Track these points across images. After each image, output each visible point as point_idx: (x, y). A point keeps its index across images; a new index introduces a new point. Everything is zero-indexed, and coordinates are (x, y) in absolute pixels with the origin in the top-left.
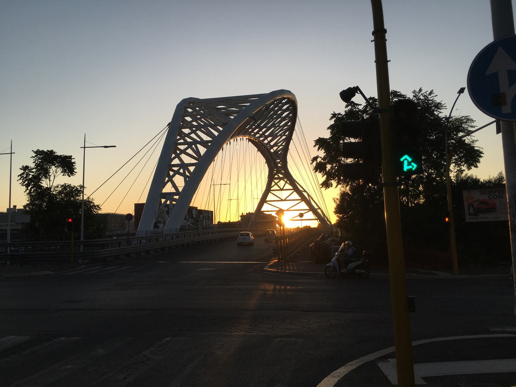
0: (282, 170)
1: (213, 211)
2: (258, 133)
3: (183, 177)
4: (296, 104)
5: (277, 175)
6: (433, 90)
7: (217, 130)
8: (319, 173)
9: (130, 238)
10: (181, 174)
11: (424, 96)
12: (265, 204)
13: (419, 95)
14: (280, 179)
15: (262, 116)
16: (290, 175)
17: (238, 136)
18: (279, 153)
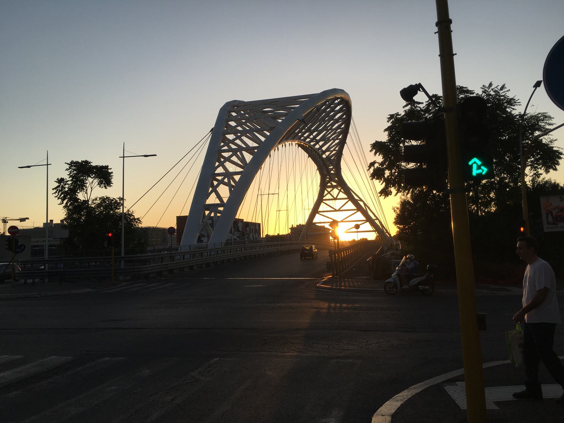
0: (335, 178)
1: (260, 224)
2: (308, 137)
3: (228, 187)
5: (330, 183)
6: (504, 84)
7: (264, 135)
8: (376, 180)
9: (173, 253)
10: (225, 184)
11: (495, 91)
12: (317, 214)
13: (489, 90)
14: (333, 187)
17: (287, 141)
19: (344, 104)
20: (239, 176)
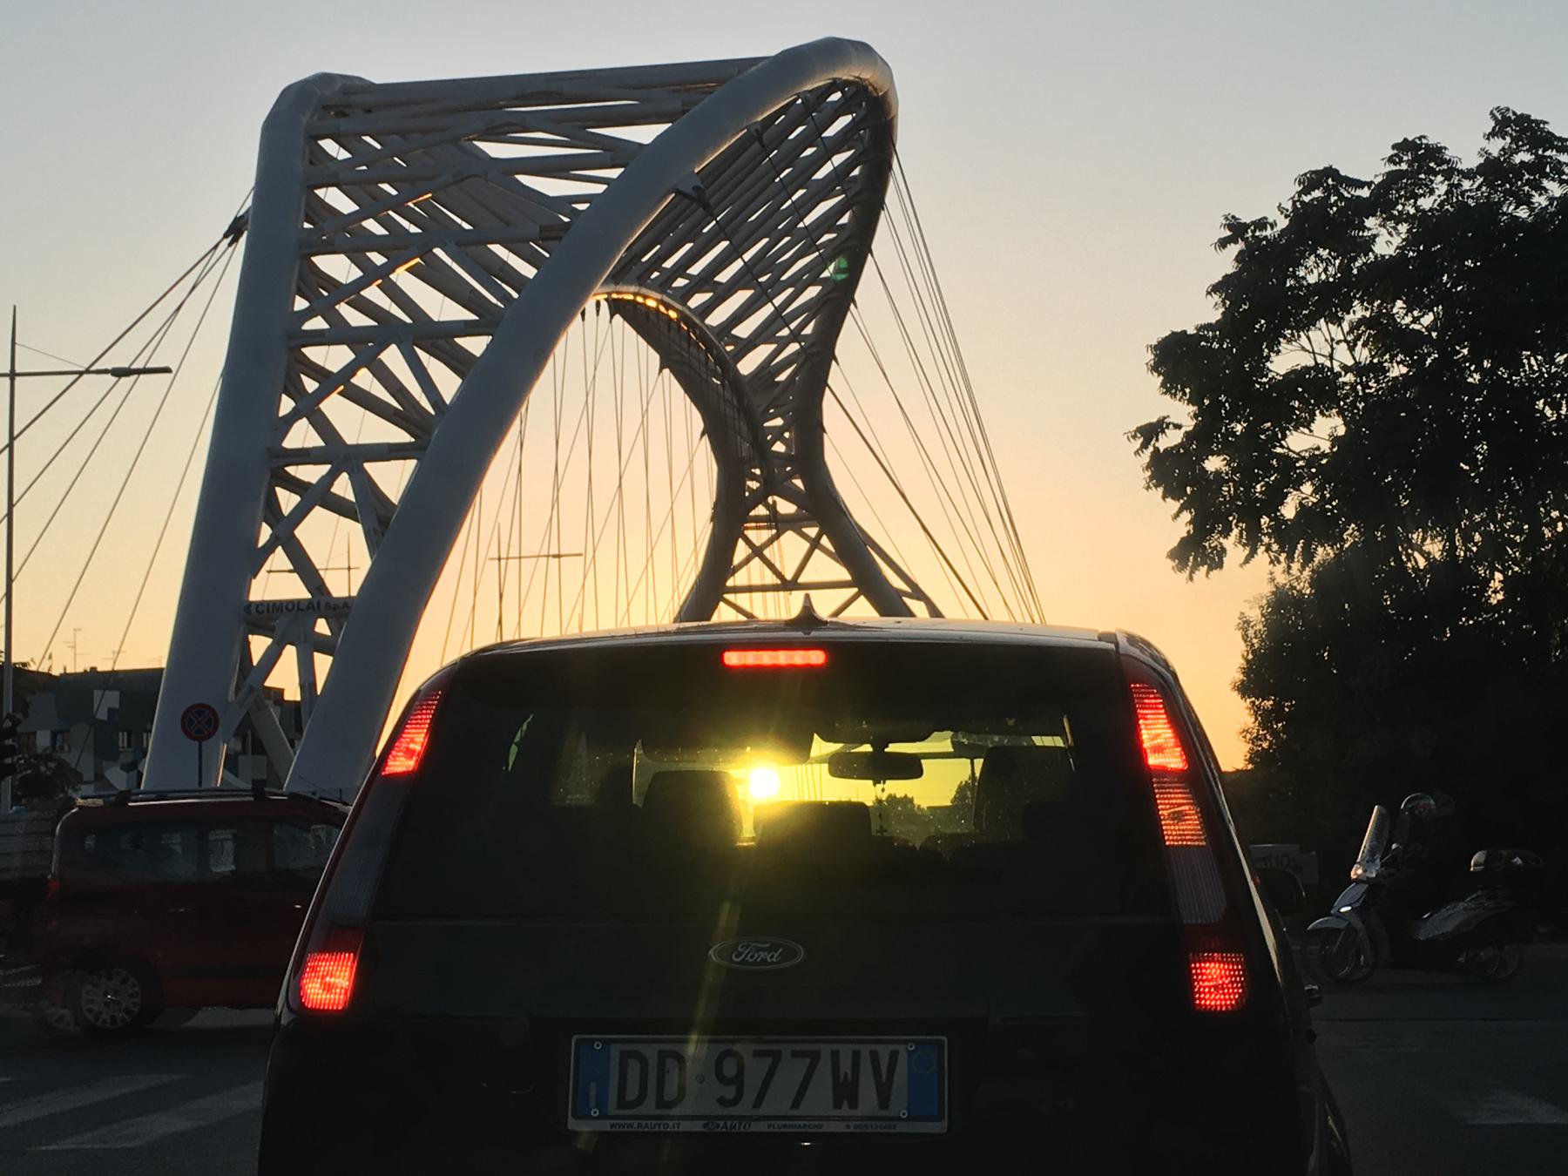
0: (791, 476)
2: (681, 269)
4: (889, 113)
5: (767, 506)
14: (779, 524)
15: (740, 188)
16: (841, 507)
18: (782, 377)
19: (863, 113)
20: (411, 464)
